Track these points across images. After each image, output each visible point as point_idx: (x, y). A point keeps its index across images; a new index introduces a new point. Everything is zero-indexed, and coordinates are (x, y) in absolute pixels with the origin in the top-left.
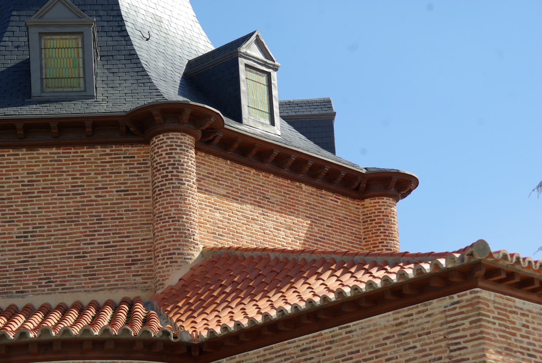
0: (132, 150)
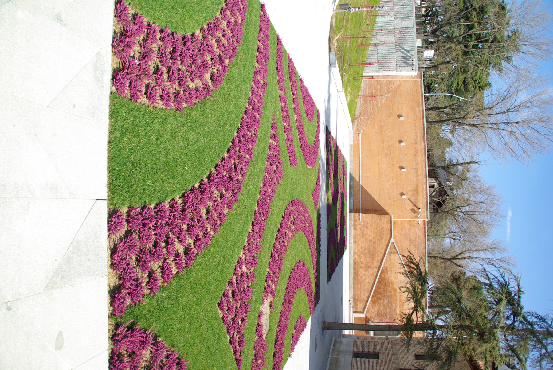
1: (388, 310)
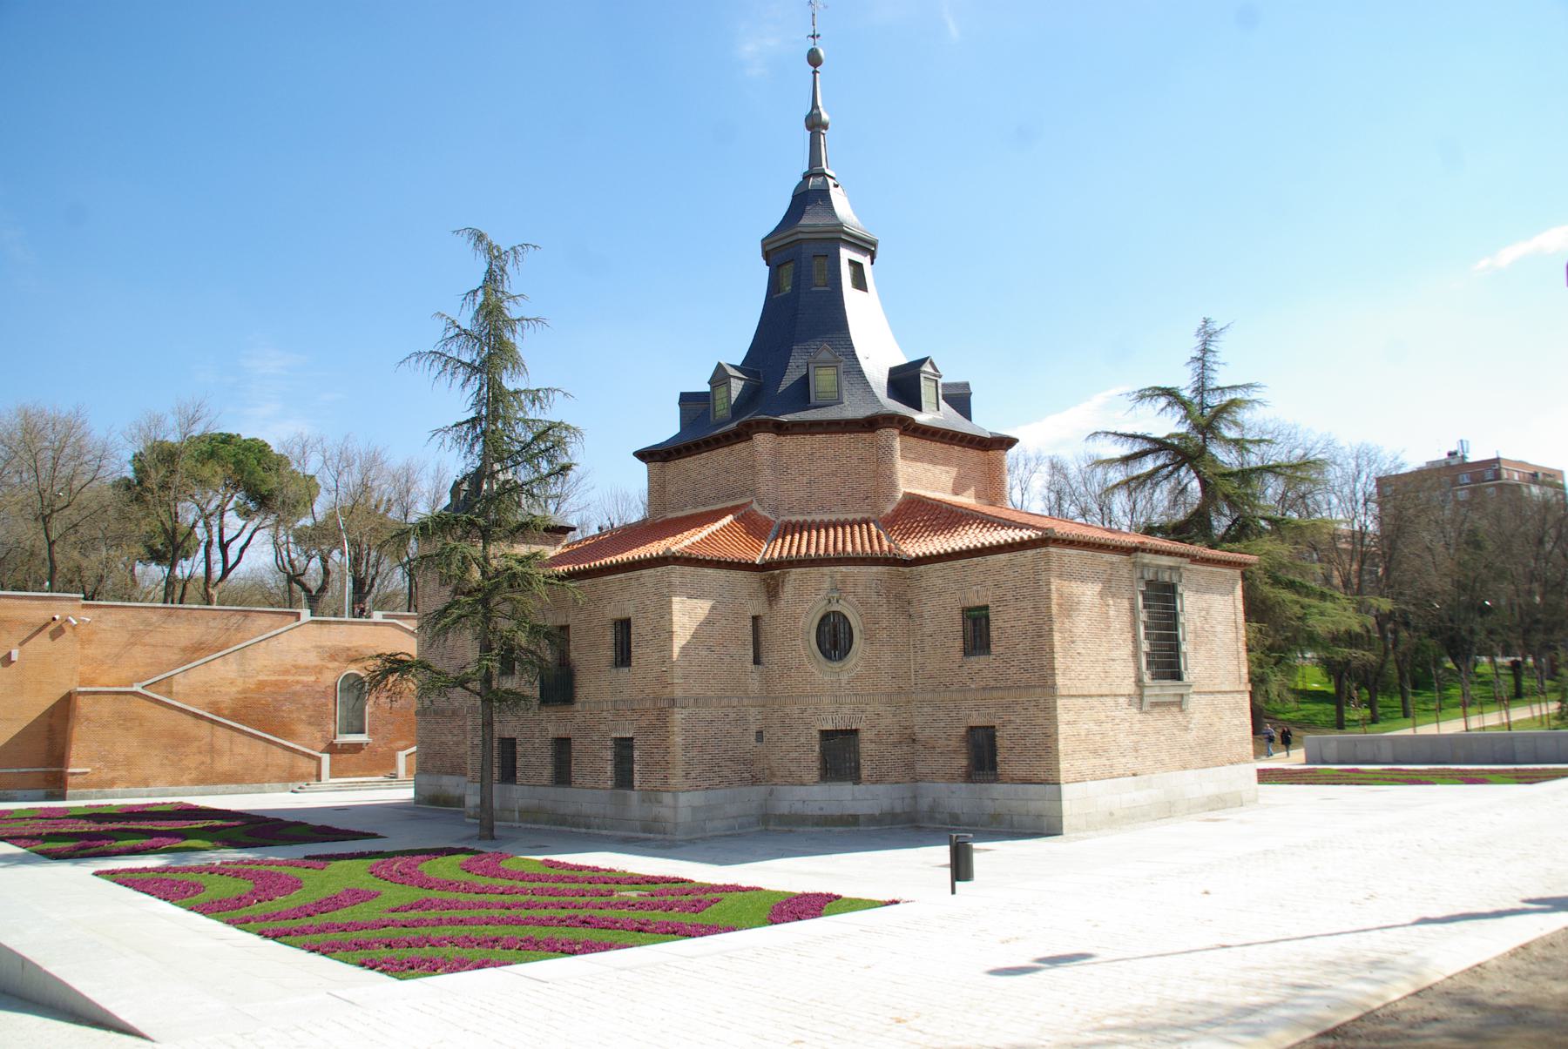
0: (865, 435)
1: (308, 702)
